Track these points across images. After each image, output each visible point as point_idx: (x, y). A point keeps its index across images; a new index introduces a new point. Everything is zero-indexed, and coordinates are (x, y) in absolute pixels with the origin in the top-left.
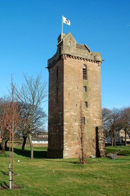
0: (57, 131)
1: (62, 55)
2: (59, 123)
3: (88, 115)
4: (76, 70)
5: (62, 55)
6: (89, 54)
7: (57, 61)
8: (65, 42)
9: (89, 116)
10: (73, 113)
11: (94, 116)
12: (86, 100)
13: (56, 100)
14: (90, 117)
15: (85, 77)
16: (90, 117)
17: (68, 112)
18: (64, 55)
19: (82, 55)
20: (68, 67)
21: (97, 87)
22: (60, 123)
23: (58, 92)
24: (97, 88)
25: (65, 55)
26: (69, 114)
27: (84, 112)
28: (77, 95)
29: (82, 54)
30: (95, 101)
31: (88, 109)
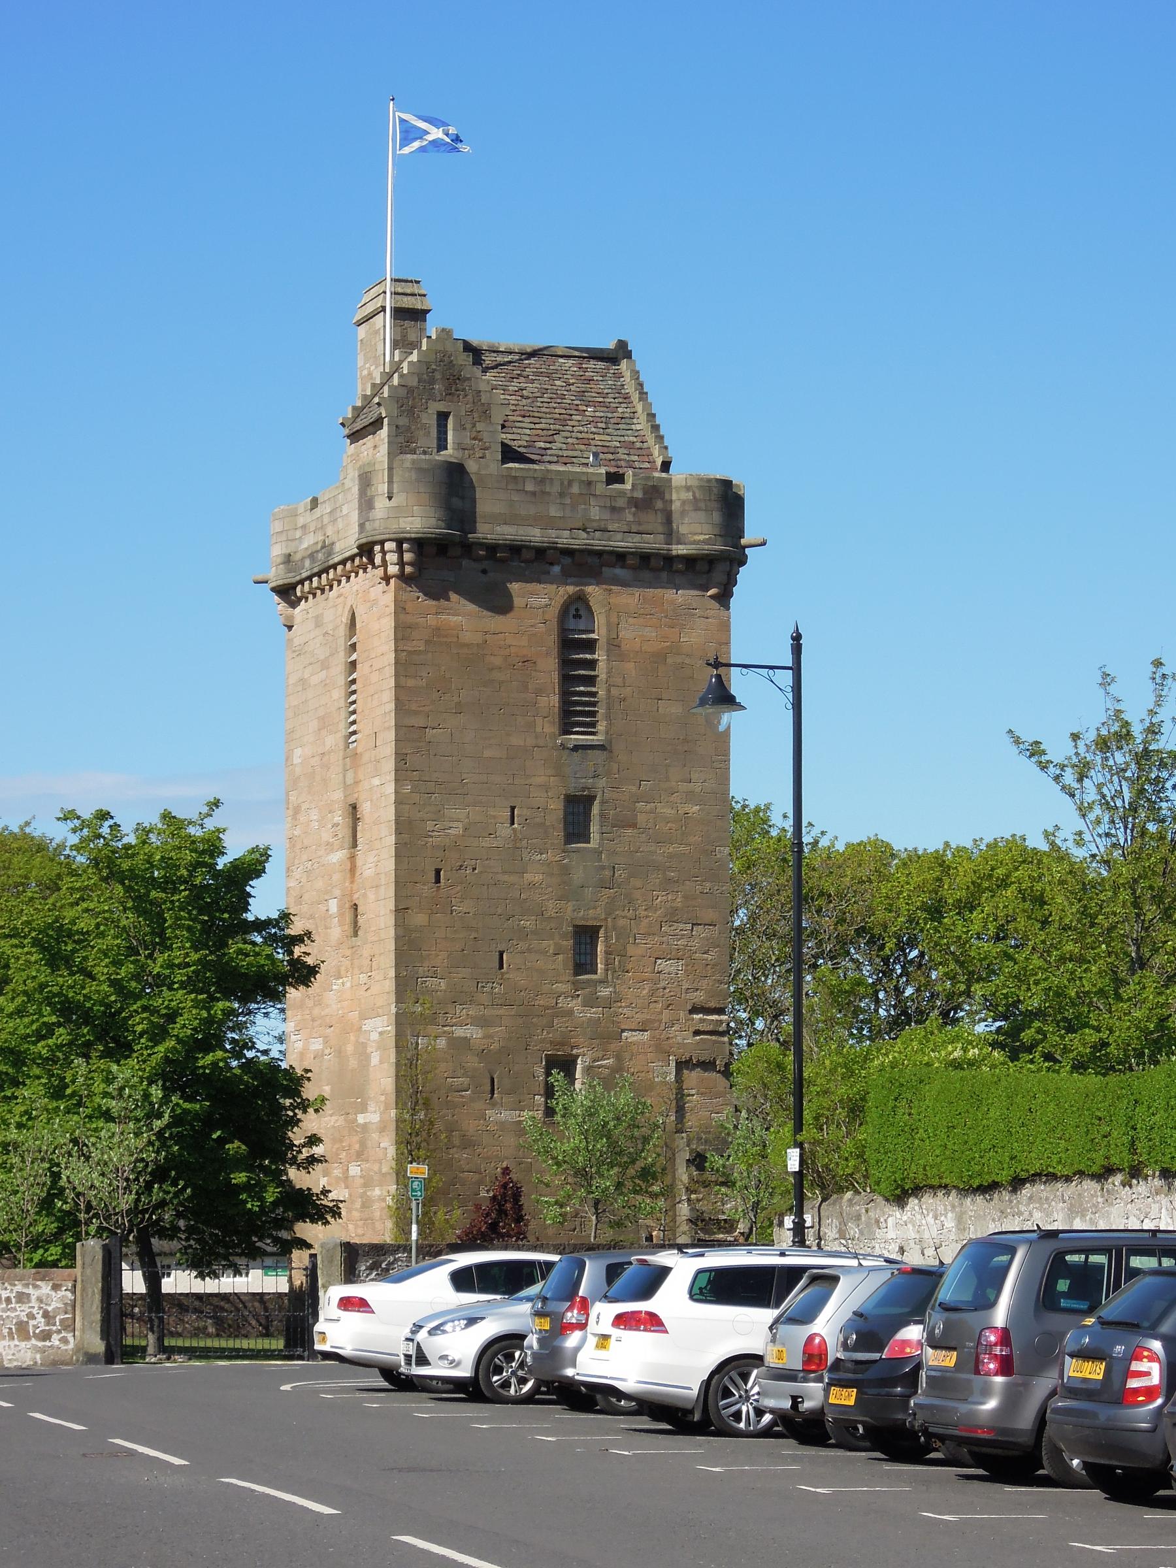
0: (354, 1170)
1: (382, 543)
2: (363, 1109)
3: (607, 1036)
4: (498, 661)
5: (382, 543)
6: (621, 503)
7: (343, 562)
8: (403, 421)
9: (614, 1046)
10: (473, 1033)
11: (661, 1049)
12: (590, 916)
13: (340, 907)
14: (619, 1058)
15: (573, 714)
16: (619, 1058)
17: (432, 1020)
18: (389, 546)
19: (548, 523)
20: (428, 642)
21: (697, 787)
22: (372, 1106)
23: (354, 844)
24: (690, 797)
25: (400, 542)
26: (442, 1043)
27: (570, 1013)
28: (506, 878)
29: (554, 511)
30: (672, 916)
31: (604, 992)
